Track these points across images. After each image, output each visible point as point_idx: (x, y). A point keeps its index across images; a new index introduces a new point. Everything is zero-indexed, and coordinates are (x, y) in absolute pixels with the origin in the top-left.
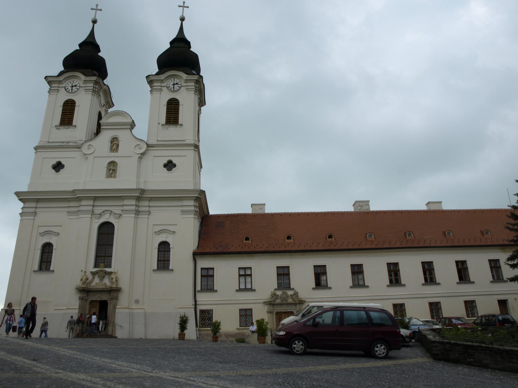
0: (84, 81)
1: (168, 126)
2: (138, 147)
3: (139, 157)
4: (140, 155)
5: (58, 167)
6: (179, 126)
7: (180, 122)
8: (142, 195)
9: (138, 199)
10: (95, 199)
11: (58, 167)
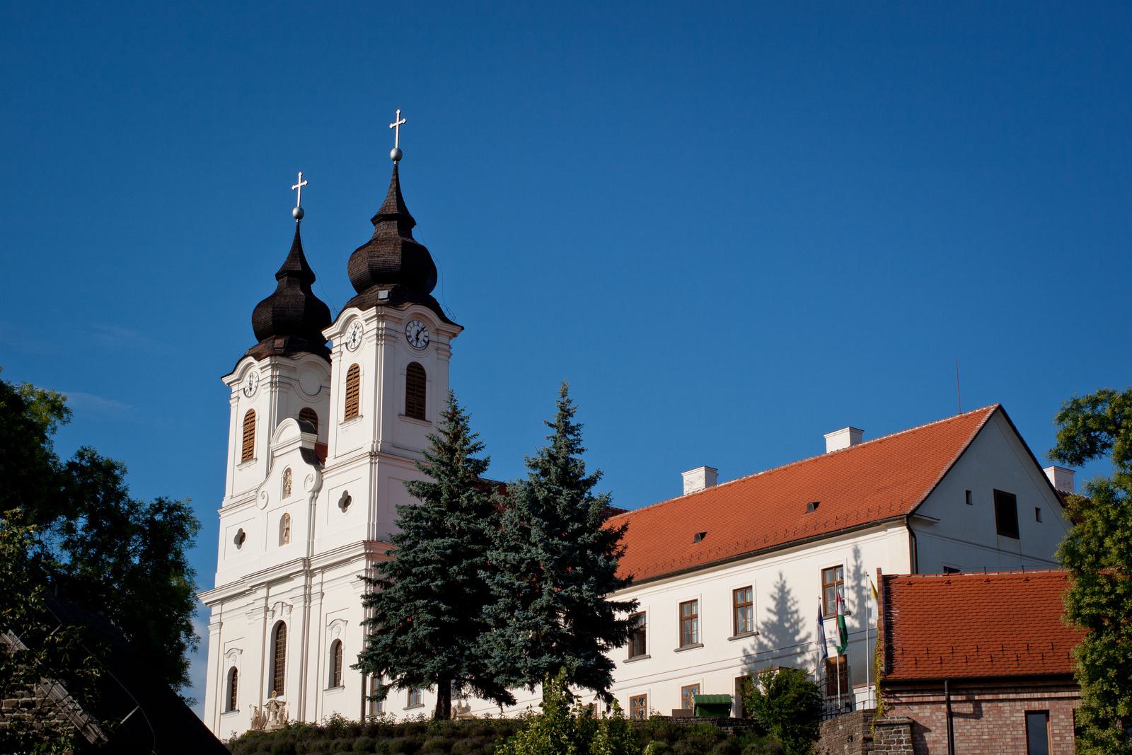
0: (261, 369)
1: (346, 424)
2: (309, 481)
3: (312, 498)
4: (310, 494)
5: (241, 538)
6: (358, 419)
7: (360, 414)
8: (309, 567)
9: (310, 573)
10: (270, 584)
11: (241, 538)
